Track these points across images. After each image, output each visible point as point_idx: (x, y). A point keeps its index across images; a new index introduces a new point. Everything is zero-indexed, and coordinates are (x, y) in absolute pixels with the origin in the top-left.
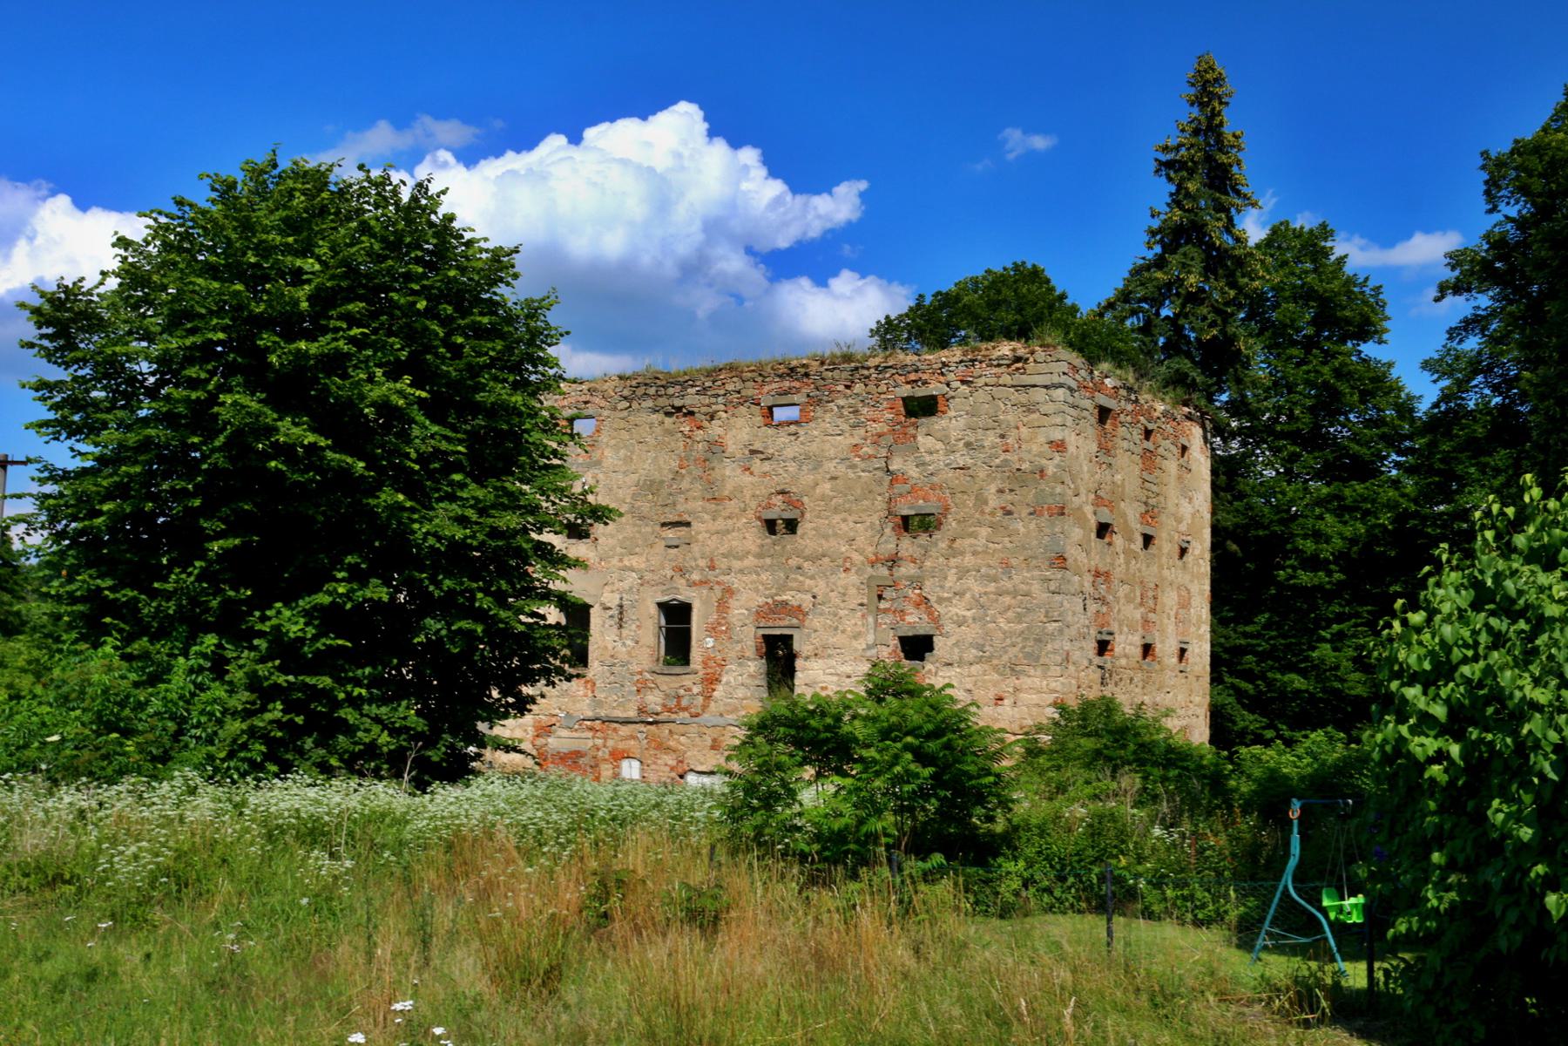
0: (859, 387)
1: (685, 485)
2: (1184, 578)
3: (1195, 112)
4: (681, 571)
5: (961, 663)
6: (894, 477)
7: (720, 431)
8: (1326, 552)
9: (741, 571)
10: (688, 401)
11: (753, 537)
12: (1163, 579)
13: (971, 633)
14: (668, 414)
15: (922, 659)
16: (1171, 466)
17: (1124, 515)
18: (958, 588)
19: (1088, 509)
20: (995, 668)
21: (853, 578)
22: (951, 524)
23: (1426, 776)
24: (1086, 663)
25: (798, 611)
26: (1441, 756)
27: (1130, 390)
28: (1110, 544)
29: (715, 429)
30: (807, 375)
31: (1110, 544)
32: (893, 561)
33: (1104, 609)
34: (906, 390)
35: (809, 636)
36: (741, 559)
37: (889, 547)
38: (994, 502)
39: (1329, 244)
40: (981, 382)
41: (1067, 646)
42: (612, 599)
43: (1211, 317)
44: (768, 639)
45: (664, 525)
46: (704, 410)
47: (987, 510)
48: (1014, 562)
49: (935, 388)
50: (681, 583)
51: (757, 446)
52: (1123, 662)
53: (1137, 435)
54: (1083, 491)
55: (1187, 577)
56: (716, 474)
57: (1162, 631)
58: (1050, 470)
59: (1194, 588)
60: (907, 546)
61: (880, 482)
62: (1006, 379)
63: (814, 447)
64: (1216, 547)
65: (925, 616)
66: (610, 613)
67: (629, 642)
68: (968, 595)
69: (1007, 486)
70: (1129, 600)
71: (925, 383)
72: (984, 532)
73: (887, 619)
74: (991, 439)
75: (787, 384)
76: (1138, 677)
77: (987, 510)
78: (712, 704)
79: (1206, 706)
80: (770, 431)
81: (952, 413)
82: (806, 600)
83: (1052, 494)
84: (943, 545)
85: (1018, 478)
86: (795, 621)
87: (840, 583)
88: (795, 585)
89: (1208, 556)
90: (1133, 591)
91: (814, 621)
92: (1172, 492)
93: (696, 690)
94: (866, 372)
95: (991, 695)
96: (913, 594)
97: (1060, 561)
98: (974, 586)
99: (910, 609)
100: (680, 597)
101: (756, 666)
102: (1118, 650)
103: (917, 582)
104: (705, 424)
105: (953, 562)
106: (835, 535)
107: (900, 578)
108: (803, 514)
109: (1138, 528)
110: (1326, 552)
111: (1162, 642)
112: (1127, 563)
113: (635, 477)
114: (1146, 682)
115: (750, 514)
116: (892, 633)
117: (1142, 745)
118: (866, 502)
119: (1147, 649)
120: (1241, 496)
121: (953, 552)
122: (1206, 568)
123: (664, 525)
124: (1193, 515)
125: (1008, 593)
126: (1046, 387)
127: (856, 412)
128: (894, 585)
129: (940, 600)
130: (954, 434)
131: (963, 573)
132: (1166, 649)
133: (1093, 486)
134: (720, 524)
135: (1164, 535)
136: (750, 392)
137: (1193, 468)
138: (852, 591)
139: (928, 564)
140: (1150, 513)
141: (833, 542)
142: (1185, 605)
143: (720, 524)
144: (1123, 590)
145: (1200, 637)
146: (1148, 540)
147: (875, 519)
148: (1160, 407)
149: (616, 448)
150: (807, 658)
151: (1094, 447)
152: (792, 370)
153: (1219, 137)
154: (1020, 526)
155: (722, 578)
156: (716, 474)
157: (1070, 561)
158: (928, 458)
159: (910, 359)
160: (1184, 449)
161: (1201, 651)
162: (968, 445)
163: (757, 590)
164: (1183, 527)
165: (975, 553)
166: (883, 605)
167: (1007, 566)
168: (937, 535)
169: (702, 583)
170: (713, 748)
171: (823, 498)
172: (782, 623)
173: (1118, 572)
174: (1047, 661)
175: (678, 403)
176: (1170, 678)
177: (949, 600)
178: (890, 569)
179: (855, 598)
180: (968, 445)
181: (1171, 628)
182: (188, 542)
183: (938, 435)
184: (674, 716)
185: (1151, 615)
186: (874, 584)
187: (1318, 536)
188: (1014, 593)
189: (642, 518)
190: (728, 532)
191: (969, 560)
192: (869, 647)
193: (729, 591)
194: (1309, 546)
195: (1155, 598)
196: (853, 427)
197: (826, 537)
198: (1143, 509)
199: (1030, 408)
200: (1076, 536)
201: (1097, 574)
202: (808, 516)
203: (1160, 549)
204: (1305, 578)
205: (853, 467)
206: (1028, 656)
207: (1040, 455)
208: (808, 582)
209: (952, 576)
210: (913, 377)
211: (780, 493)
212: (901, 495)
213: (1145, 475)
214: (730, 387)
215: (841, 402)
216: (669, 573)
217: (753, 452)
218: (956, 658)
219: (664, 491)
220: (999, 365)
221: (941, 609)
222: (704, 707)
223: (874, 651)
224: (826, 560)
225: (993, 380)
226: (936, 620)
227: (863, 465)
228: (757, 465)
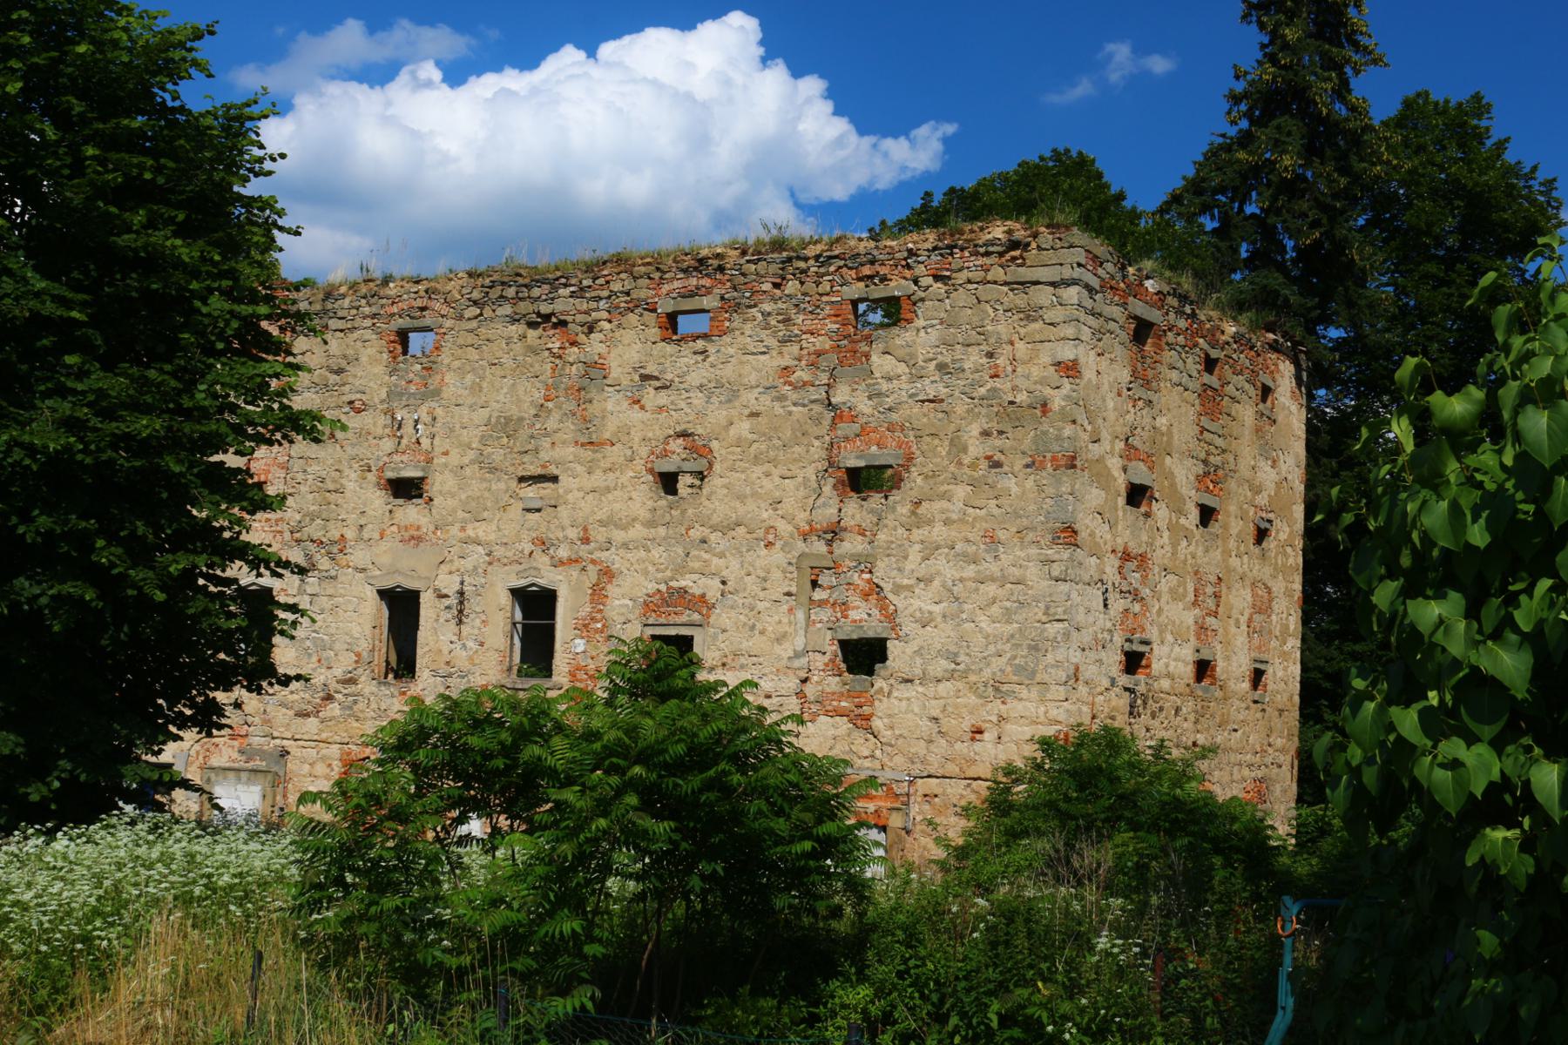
0: (792, 287)
1: (552, 424)
2: (1262, 571)
4: (543, 544)
5: (923, 680)
7: (602, 348)
9: (625, 546)
10: (558, 306)
11: (642, 498)
12: (1229, 570)
13: (939, 636)
14: (532, 325)
15: (870, 673)
17: (1170, 476)
18: (922, 572)
19: (1114, 464)
20: (973, 687)
21: (778, 557)
22: (915, 481)
23: (1471, 859)
24: (1106, 683)
25: (701, 603)
26: (1505, 801)
27: (1183, 298)
28: (1147, 515)
29: (594, 345)
30: (721, 269)
31: (1147, 515)
32: (834, 533)
33: (1137, 607)
35: (715, 637)
36: (625, 528)
37: (827, 513)
39: (1484, 123)
40: (962, 277)
41: (1076, 657)
42: (450, 584)
43: (1313, 215)
45: (522, 479)
46: (580, 318)
47: (967, 460)
48: (1002, 535)
49: (898, 286)
50: (542, 560)
51: (651, 369)
52: (1165, 684)
53: (1193, 364)
54: (1105, 435)
55: (1268, 570)
56: (593, 409)
57: (1226, 643)
58: (1057, 403)
59: (1278, 586)
60: (855, 511)
61: (817, 421)
62: (997, 273)
63: (728, 372)
65: (875, 612)
66: (447, 602)
67: (470, 644)
68: (936, 583)
69: (994, 426)
70: (1176, 596)
71: (884, 279)
73: (824, 614)
74: (974, 358)
75: (694, 281)
76: (1188, 707)
77: (967, 460)
79: (1293, 752)
80: (670, 349)
81: (920, 323)
82: (712, 588)
83: (1059, 438)
84: (903, 510)
85: (1011, 414)
86: (696, 617)
87: (757, 564)
88: (697, 565)
89: (1299, 543)
90: (1183, 584)
91: (721, 617)
92: (1247, 452)
94: (802, 265)
95: (967, 725)
97: (1068, 534)
98: (945, 568)
99: (855, 600)
100: (542, 582)
102: (1157, 667)
103: (866, 564)
104: (582, 338)
105: (917, 534)
106: (755, 495)
107: (843, 557)
108: (711, 465)
109: (1191, 496)
111: (1227, 658)
112: (1175, 545)
113: (485, 413)
114: (1199, 717)
115: (639, 464)
116: (829, 634)
118: (797, 449)
119: (1203, 669)
121: (917, 520)
122: (1296, 559)
123: (522, 479)
124: (1278, 485)
125: (993, 580)
126: (1053, 284)
127: (787, 321)
128: (834, 567)
129: (898, 589)
130: (922, 353)
132: (1234, 666)
133: (1122, 430)
134: (598, 479)
135: (1233, 508)
136: (643, 294)
137: (1280, 419)
138: (776, 575)
139: (882, 537)
140: (1211, 476)
141: (751, 505)
142: (1263, 607)
143: (598, 479)
144: (1166, 583)
145: (1285, 656)
146: (1207, 515)
147: (810, 473)
148: (1231, 329)
149: (462, 373)
151: (1125, 375)
152: (702, 261)
154: (1011, 484)
155: (597, 555)
157: (1083, 535)
158: (885, 386)
160: (1266, 392)
161: (1286, 675)
162: (941, 367)
163: (646, 573)
164: (1262, 500)
165: (947, 522)
166: (818, 595)
167: (992, 540)
168: (895, 496)
169: (571, 561)
172: (679, 620)
173: (1160, 556)
174: (1046, 678)
175: (545, 308)
176: (1238, 710)
177: (909, 588)
178: (829, 543)
179: (779, 584)
180: (941, 367)
181: (1240, 640)
183: (901, 353)
185: (1210, 621)
186: (806, 564)
188: (1003, 581)
189: (493, 470)
190: (608, 490)
191: (938, 532)
192: (797, 655)
193: (607, 574)
195: (1217, 596)
196: (783, 342)
197: (741, 498)
198: (1200, 469)
199: (1030, 314)
200: (1094, 504)
201: (1126, 556)
202: (717, 467)
203: (1226, 527)
205: (781, 398)
206: (1019, 670)
207: (1043, 381)
208: (715, 560)
209: (915, 553)
210: (867, 271)
212: (847, 439)
213: (1205, 421)
214: (616, 287)
215: (767, 307)
216: (528, 547)
217: (645, 378)
218: (918, 672)
219: (524, 433)
220: (987, 254)
223: (804, 661)
224: (741, 530)
225: (979, 275)
226: (891, 617)
227: (794, 396)
228: (651, 397)
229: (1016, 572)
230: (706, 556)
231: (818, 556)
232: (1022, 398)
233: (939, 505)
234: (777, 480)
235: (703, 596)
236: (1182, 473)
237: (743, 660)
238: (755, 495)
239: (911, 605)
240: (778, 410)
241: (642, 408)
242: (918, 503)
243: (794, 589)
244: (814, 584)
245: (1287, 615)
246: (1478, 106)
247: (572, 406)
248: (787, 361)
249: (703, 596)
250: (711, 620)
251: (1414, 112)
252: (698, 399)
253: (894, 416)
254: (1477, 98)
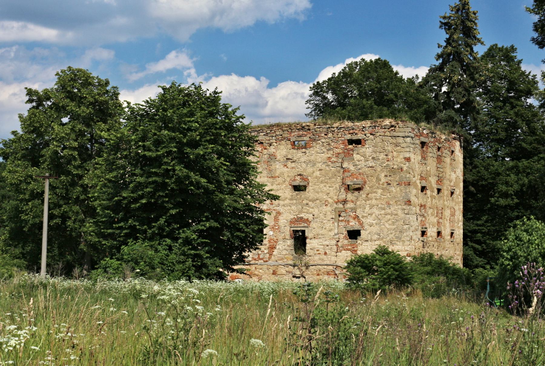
0: (330, 135)
2: (452, 204)
5: (371, 240)
6: (345, 170)
7: (274, 150)
8: (511, 191)
9: (284, 205)
12: (444, 205)
13: (375, 229)
15: (356, 239)
16: (448, 160)
17: (430, 182)
18: (370, 212)
19: (418, 182)
21: (329, 208)
22: (367, 188)
24: (418, 240)
26: (509, 265)
27: (433, 133)
28: (426, 194)
29: (272, 150)
30: (309, 129)
31: (426, 194)
32: (345, 202)
33: (424, 219)
34: (349, 137)
35: (312, 230)
37: (343, 196)
38: (383, 180)
39: (515, 54)
40: (378, 134)
41: (411, 234)
43: (463, 92)
44: (295, 232)
46: (267, 142)
47: (381, 183)
48: (391, 203)
49: (360, 136)
51: (289, 157)
52: (430, 239)
53: (435, 150)
54: (416, 175)
55: (454, 204)
56: (273, 167)
57: (444, 226)
58: (405, 168)
59: (456, 208)
60: (350, 196)
61: (339, 172)
62: (388, 134)
63: (312, 158)
64: (465, 187)
65: (357, 223)
68: (374, 215)
69: (388, 174)
70: (432, 215)
71: (356, 134)
72: (380, 191)
73: (343, 224)
74: (382, 156)
75: (301, 133)
76: (436, 244)
77: (381, 183)
78: (273, 257)
79: (461, 255)
80: (295, 151)
81: (367, 146)
82: (310, 217)
83: (406, 178)
84: (364, 196)
85: (393, 171)
86: (306, 225)
87: (323, 210)
88: (305, 211)
89: (462, 194)
90: (434, 211)
91: (313, 225)
92: (448, 170)
93: (266, 251)
94: (333, 129)
96: (352, 214)
97: (409, 202)
98: (376, 211)
99: (351, 220)
101: (290, 242)
102: (429, 234)
103: (354, 210)
104: (268, 147)
105: (368, 202)
106: (322, 192)
107: (348, 208)
108: (308, 183)
109: (435, 186)
110: (511, 191)
111: (445, 230)
112: (432, 201)
114: (438, 246)
115: (287, 183)
116: (344, 229)
117: (446, 268)
118: (333, 179)
119: (439, 233)
120: (476, 167)
121: (368, 198)
122: (461, 199)
124: (456, 178)
125: (389, 214)
126: (403, 137)
127: (329, 144)
128: (345, 211)
129: (363, 217)
130: (368, 154)
131: (372, 207)
132: (446, 233)
133: (419, 173)
135: (445, 188)
136: (286, 136)
137: (456, 159)
138: (329, 213)
139: (358, 203)
140: (440, 180)
141: (321, 194)
142: (453, 215)
144: (430, 211)
145: (459, 227)
146: (439, 190)
148: (443, 137)
150: (311, 239)
151: (420, 158)
152: (303, 127)
153: (467, 14)
154: (393, 189)
155: (275, 208)
156: (273, 167)
157: (412, 202)
158: (358, 163)
159: (350, 124)
160: (453, 152)
161: (459, 233)
162: (373, 158)
163: (290, 213)
164: (452, 184)
165: (376, 199)
166: (341, 218)
167: (388, 204)
170: (273, 274)
171: (316, 177)
173: (428, 205)
174: (404, 239)
176: (447, 244)
177: (366, 217)
178: (343, 205)
180: (373, 158)
181: (448, 225)
182: (162, 210)
183: (362, 154)
184: (257, 262)
185: (441, 220)
186: (337, 210)
187: (507, 183)
188: (391, 214)
191: (374, 202)
192: (335, 235)
193: (279, 213)
194: (504, 188)
195: (442, 213)
197: (318, 193)
198: (437, 179)
199: (397, 145)
200: (414, 191)
201: (421, 206)
202: (310, 184)
203: (443, 194)
204: (502, 202)
205: (328, 166)
206: (397, 237)
207: (401, 163)
208: (311, 209)
209: (367, 208)
210: (351, 131)
211: (298, 175)
212: (347, 177)
213: (438, 166)
214: (278, 133)
215: (323, 140)
217: (288, 159)
218: (369, 238)
220: (385, 128)
221: (363, 220)
222: (269, 258)
223: (337, 236)
224: (318, 201)
225: (383, 134)
226: (361, 224)
227: (332, 165)
228: (289, 164)
229: (395, 212)
230: (308, 208)
231: (340, 208)
232: (395, 167)
233: (374, 195)
234: (328, 188)
235: (308, 219)
236: (433, 180)
237: (320, 236)
238: (322, 192)
240: (327, 169)
241: (287, 167)
242: (368, 194)
243: (334, 217)
244: (340, 216)
245: (459, 216)
246: (513, 49)
247: (266, 166)
248: (329, 155)
249: (308, 219)
250: (311, 225)
251: (492, 53)
252: (304, 165)
253: (360, 171)
254: (512, 47)
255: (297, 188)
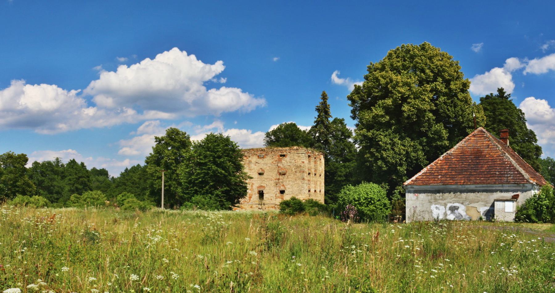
2: (320, 180)
3: (322, 101)
6: (279, 167)
8: (342, 174)
13: (291, 190)
16: (319, 162)
22: (287, 174)
25: (264, 187)
29: (250, 159)
32: (279, 179)
34: (280, 154)
37: (278, 177)
38: (294, 170)
44: (259, 191)
49: (285, 153)
60: (281, 177)
64: (325, 173)
72: (292, 175)
73: (278, 188)
74: (293, 161)
82: (265, 185)
85: (298, 167)
91: (266, 188)
92: (319, 166)
97: (304, 179)
98: (291, 183)
101: (257, 195)
103: (282, 182)
109: (314, 173)
110: (342, 174)
119: (315, 191)
120: (329, 165)
121: (288, 178)
122: (324, 178)
131: (289, 181)
132: (318, 191)
136: (256, 153)
140: (316, 170)
142: (321, 184)
146: (315, 174)
153: (326, 105)
159: (281, 149)
176: (319, 195)
179: (273, 185)
182: (207, 183)
187: (341, 172)
193: (253, 184)
194: (340, 173)
200: (306, 175)
204: (339, 179)
226: (285, 188)
228: (257, 164)
236: (313, 170)
239: (287, 187)
245: (323, 184)
246: (343, 120)
251: (336, 121)
255: (260, 174)
